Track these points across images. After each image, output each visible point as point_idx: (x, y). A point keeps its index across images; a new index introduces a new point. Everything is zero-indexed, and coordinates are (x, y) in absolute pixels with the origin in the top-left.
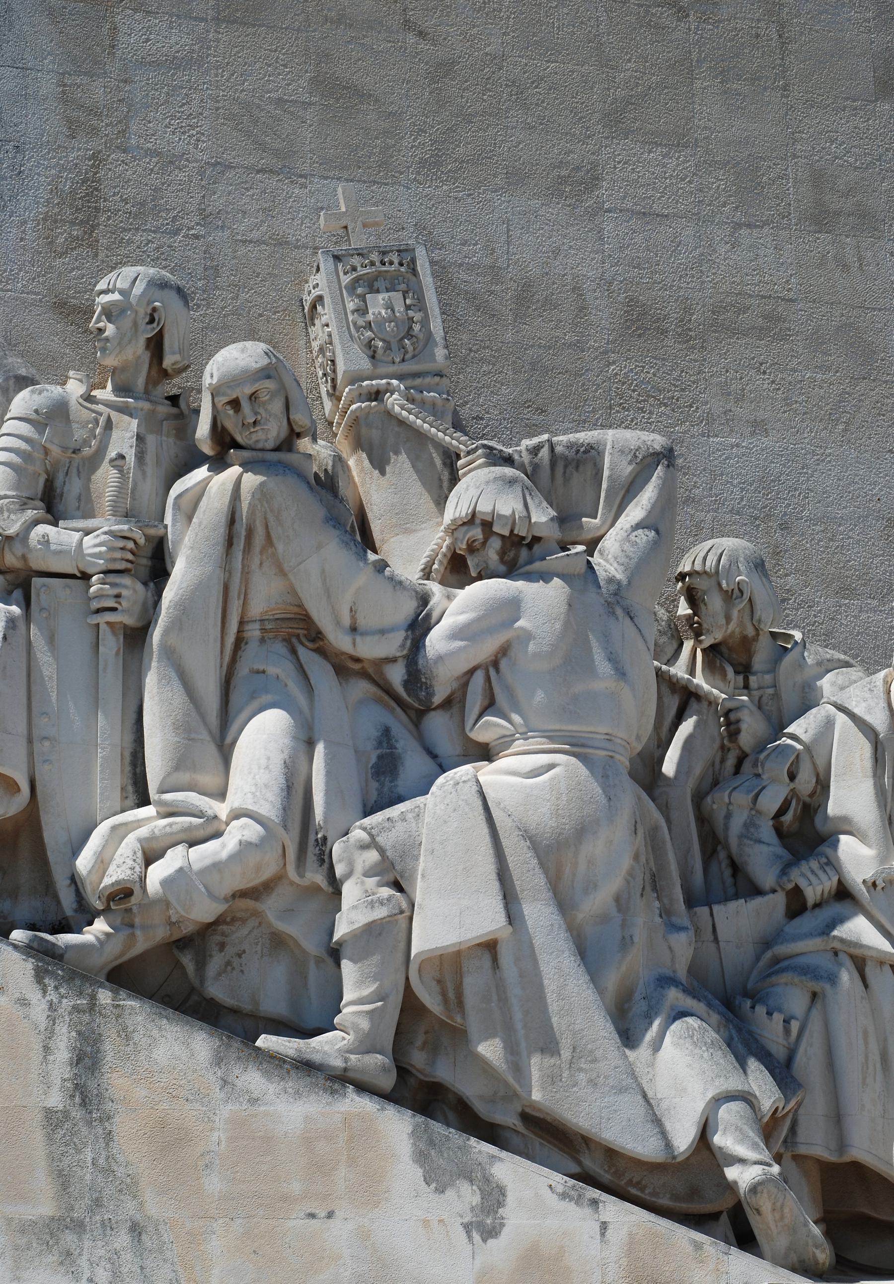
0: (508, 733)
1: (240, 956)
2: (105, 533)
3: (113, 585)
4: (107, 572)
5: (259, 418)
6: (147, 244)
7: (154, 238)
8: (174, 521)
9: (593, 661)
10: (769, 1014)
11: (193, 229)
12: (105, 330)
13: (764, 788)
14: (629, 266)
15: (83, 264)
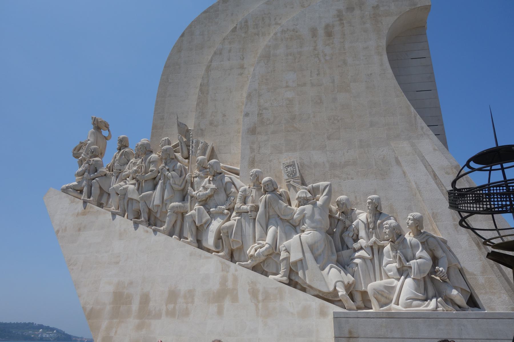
1: (269, 264)
10: (350, 268)
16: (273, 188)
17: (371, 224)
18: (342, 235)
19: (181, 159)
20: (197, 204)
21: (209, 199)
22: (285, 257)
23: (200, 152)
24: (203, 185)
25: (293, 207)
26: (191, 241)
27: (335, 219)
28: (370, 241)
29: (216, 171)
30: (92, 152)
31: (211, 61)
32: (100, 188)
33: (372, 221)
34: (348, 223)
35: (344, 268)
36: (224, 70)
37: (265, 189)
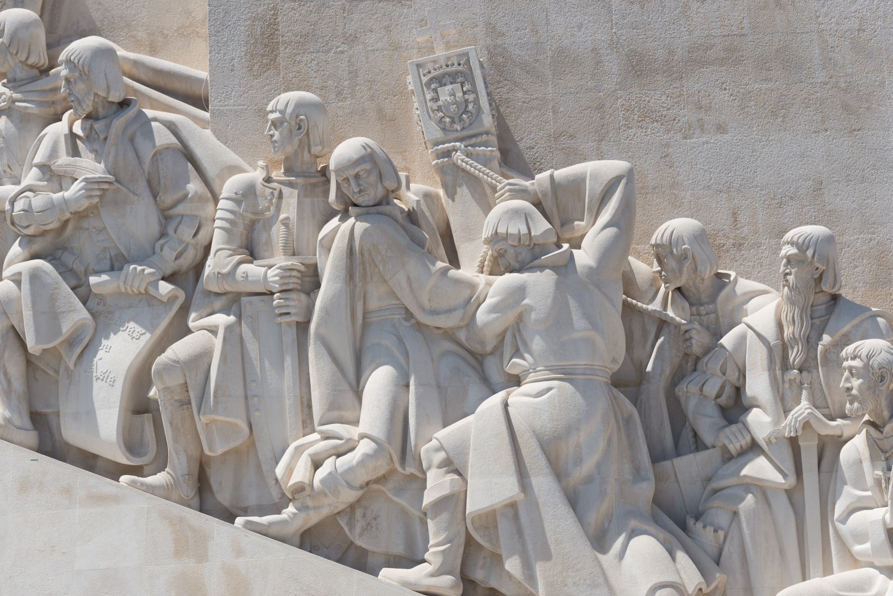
0: (526, 369)
1: (375, 519)
2: (278, 268)
3: (286, 299)
4: (280, 292)
5: (362, 188)
6: (311, 62)
7: (315, 57)
8: (320, 254)
10: (705, 527)
11: (339, 47)
12: (274, 135)
13: (707, 381)
14: (630, 29)
15: (271, 81)
16: (380, 187)
17: (795, 350)
18: (676, 389)
20: (16, 249)
21: (78, 228)
22: (445, 491)
24: (38, 159)
25: (468, 271)
28: (790, 417)
29: (102, 94)
33: (797, 336)
34: (699, 339)
35: (684, 527)
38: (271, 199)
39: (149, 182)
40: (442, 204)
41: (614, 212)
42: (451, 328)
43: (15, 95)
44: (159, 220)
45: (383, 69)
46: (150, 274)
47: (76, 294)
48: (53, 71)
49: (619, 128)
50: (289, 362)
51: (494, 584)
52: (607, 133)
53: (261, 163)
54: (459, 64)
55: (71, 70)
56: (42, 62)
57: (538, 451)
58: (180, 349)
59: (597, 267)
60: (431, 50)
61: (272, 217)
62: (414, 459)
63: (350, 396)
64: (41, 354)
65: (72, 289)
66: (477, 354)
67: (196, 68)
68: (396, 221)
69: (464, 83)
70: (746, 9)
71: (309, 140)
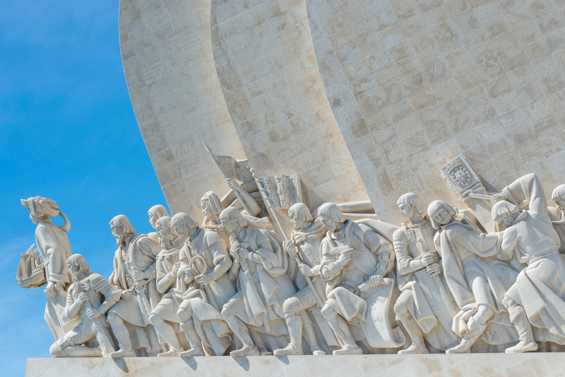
1: (495, 333)
2: (424, 258)
3: (431, 267)
4: (428, 266)
5: (443, 218)
8: (437, 247)
9: (537, 235)
19: (254, 220)
20: (328, 287)
21: (347, 271)
22: (518, 313)
23: (285, 197)
24: (324, 253)
25: (491, 233)
26: (350, 348)
27: (561, 226)
29: (338, 221)
30: (76, 268)
31: (215, 21)
32: (125, 323)
36: (247, 29)
37: (437, 221)
38: (412, 235)
39: (366, 245)
40: (472, 214)
41: (536, 192)
42: (494, 255)
43: (307, 234)
44: (374, 257)
45: (430, 175)
46: (379, 277)
47: (355, 294)
48: (315, 221)
49: (522, 163)
50: (441, 289)
51: (548, 340)
52: (519, 167)
53: (402, 224)
54: (458, 163)
55: (324, 217)
56: (311, 219)
57: (545, 286)
58: (401, 299)
59: (539, 213)
60: (445, 162)
61: (414, 241)
62: (501, 306)
63: (468, 293)
64: (352, 320)
65: (354, 293)
66: (507, 261)
67: (363, 200)
68: (459, 225)
69: (462, 168)
70: (549, 105)
71: (417, 209)
